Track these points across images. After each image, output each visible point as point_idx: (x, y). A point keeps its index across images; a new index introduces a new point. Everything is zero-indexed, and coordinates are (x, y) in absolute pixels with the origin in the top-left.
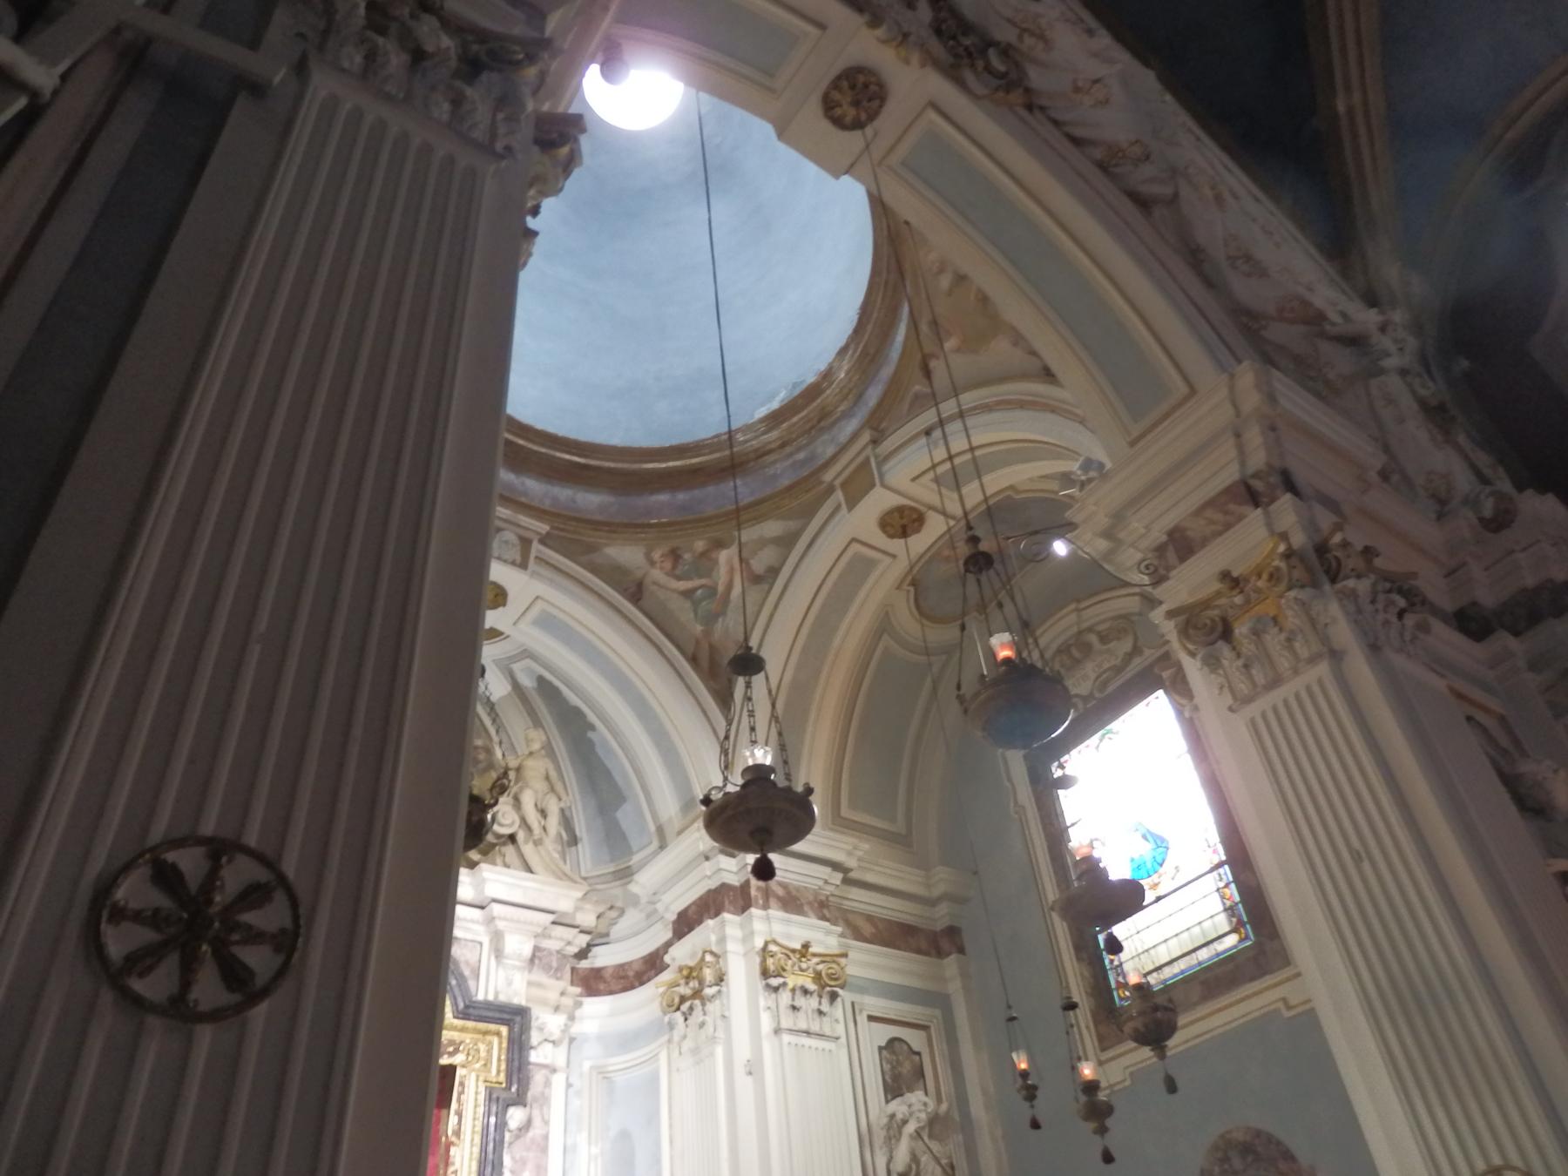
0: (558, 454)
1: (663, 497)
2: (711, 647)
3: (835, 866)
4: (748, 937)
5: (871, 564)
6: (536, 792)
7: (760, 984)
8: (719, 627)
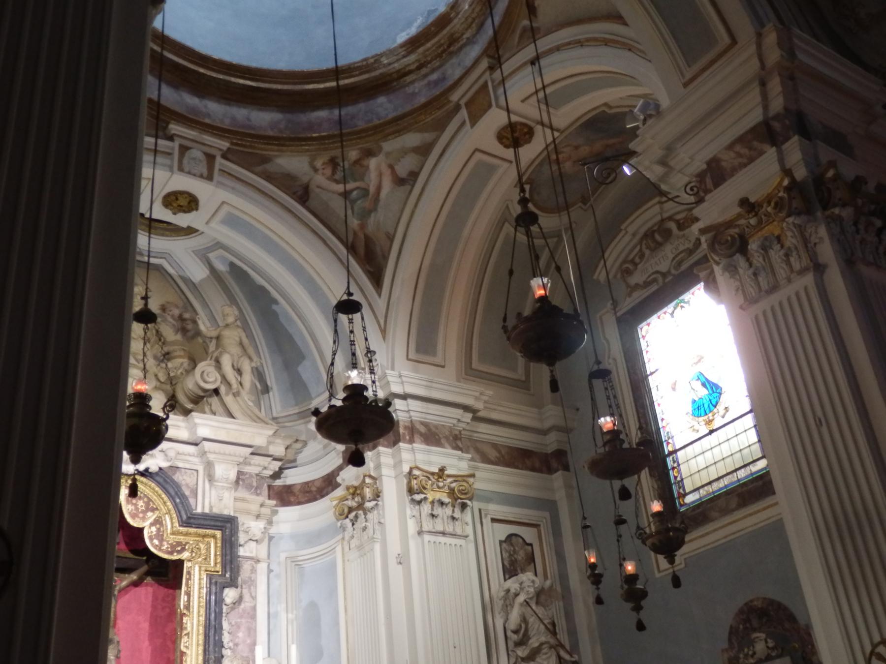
0: (233, 79)
1: (323, 114)
2: (367, 238)
3: (466, 408)
4: (398, 464)
5: (492, 169)
6: (232, 356)
7: (407, 499)
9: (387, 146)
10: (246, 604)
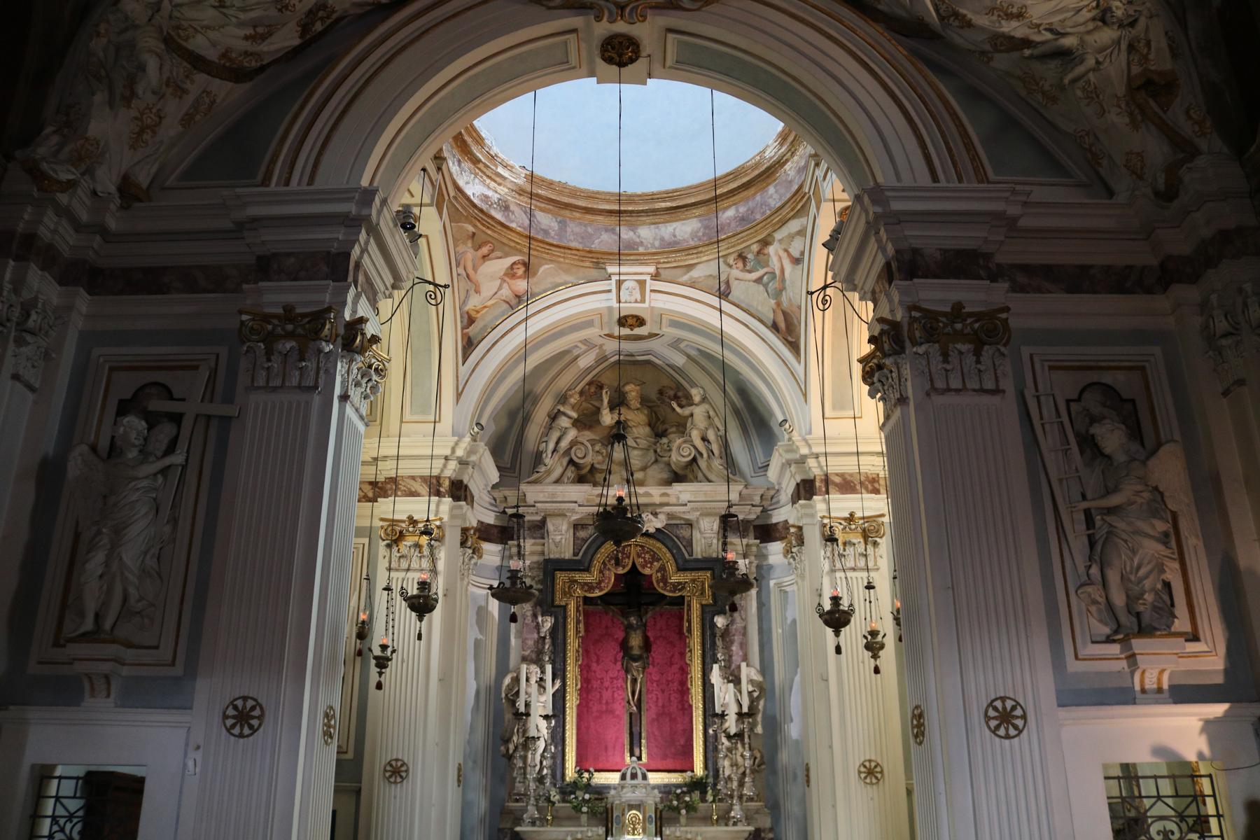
1: (731, 213)
2: (785, 314)
8: (784, 299)
9: (778, 236)
10: (739, 624)
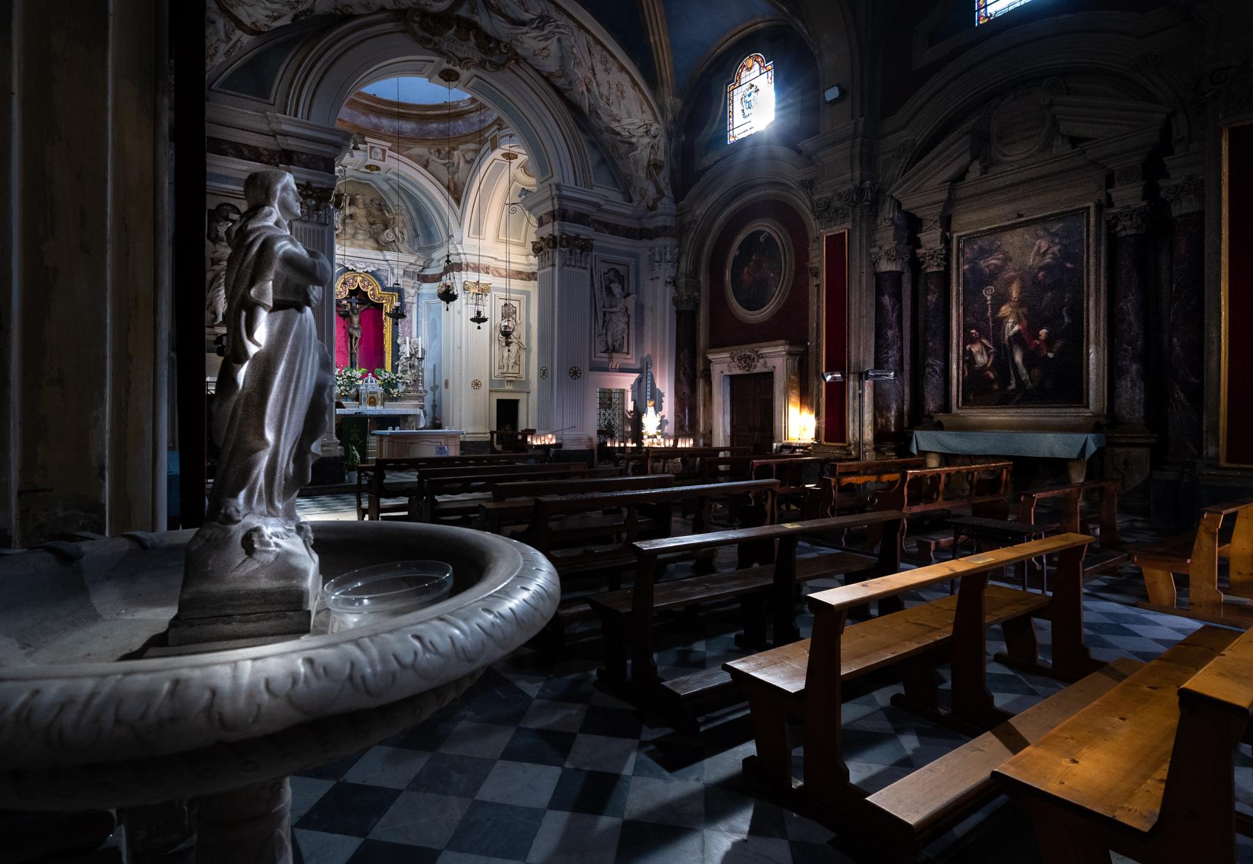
1: (434, 125)
9: (461, 147)
